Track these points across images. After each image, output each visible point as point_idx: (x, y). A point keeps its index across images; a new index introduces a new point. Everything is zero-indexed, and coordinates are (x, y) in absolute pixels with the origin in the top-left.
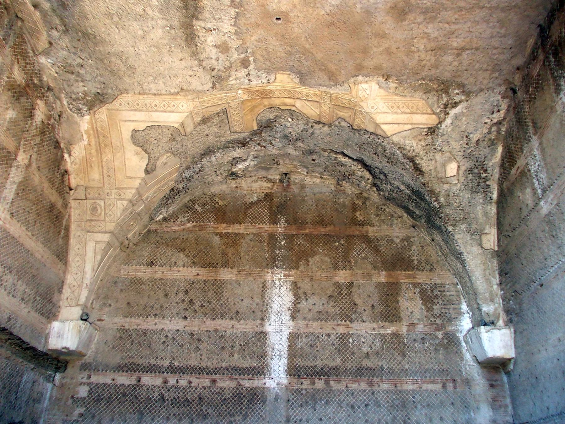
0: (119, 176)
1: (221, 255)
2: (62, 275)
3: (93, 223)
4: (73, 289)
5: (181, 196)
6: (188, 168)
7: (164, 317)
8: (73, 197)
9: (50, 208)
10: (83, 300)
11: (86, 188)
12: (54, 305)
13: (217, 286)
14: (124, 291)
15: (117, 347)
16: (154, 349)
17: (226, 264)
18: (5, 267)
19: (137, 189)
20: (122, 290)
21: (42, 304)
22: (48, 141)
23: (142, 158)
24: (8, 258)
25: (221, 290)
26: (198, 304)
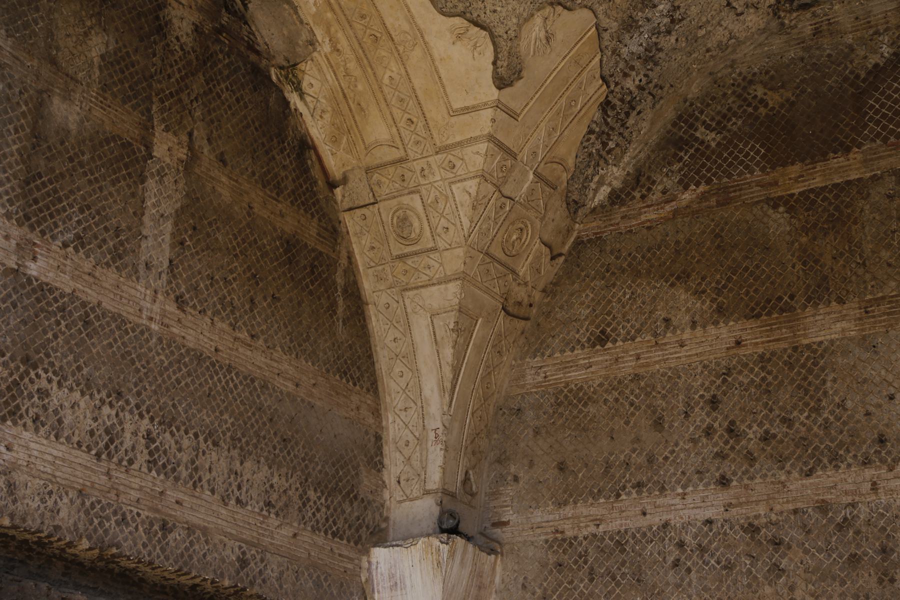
0: (436, 113)
1: (799, 266)
2: (371, 421)
3: (409, 262)
4: (407, 452)
5: (649, 115)
6: (630, 25)
7: (662, 489)
8: (346, 205)
9: (286, 251)
10: (435, 478)
11: (368, 170)
12: (366, 504)
13: (803, 366)
14: (543, 431)
15: (554, 592)
16: (654, 586)
17: (821, 291)
18: (196, 436)
19: (491, 138)
20: (537, 432)
21: (328, 507)
22: (228, 77)
23: (475, 47)
24: (199, 411)
25: (817, 377)
26: (753, 433)
